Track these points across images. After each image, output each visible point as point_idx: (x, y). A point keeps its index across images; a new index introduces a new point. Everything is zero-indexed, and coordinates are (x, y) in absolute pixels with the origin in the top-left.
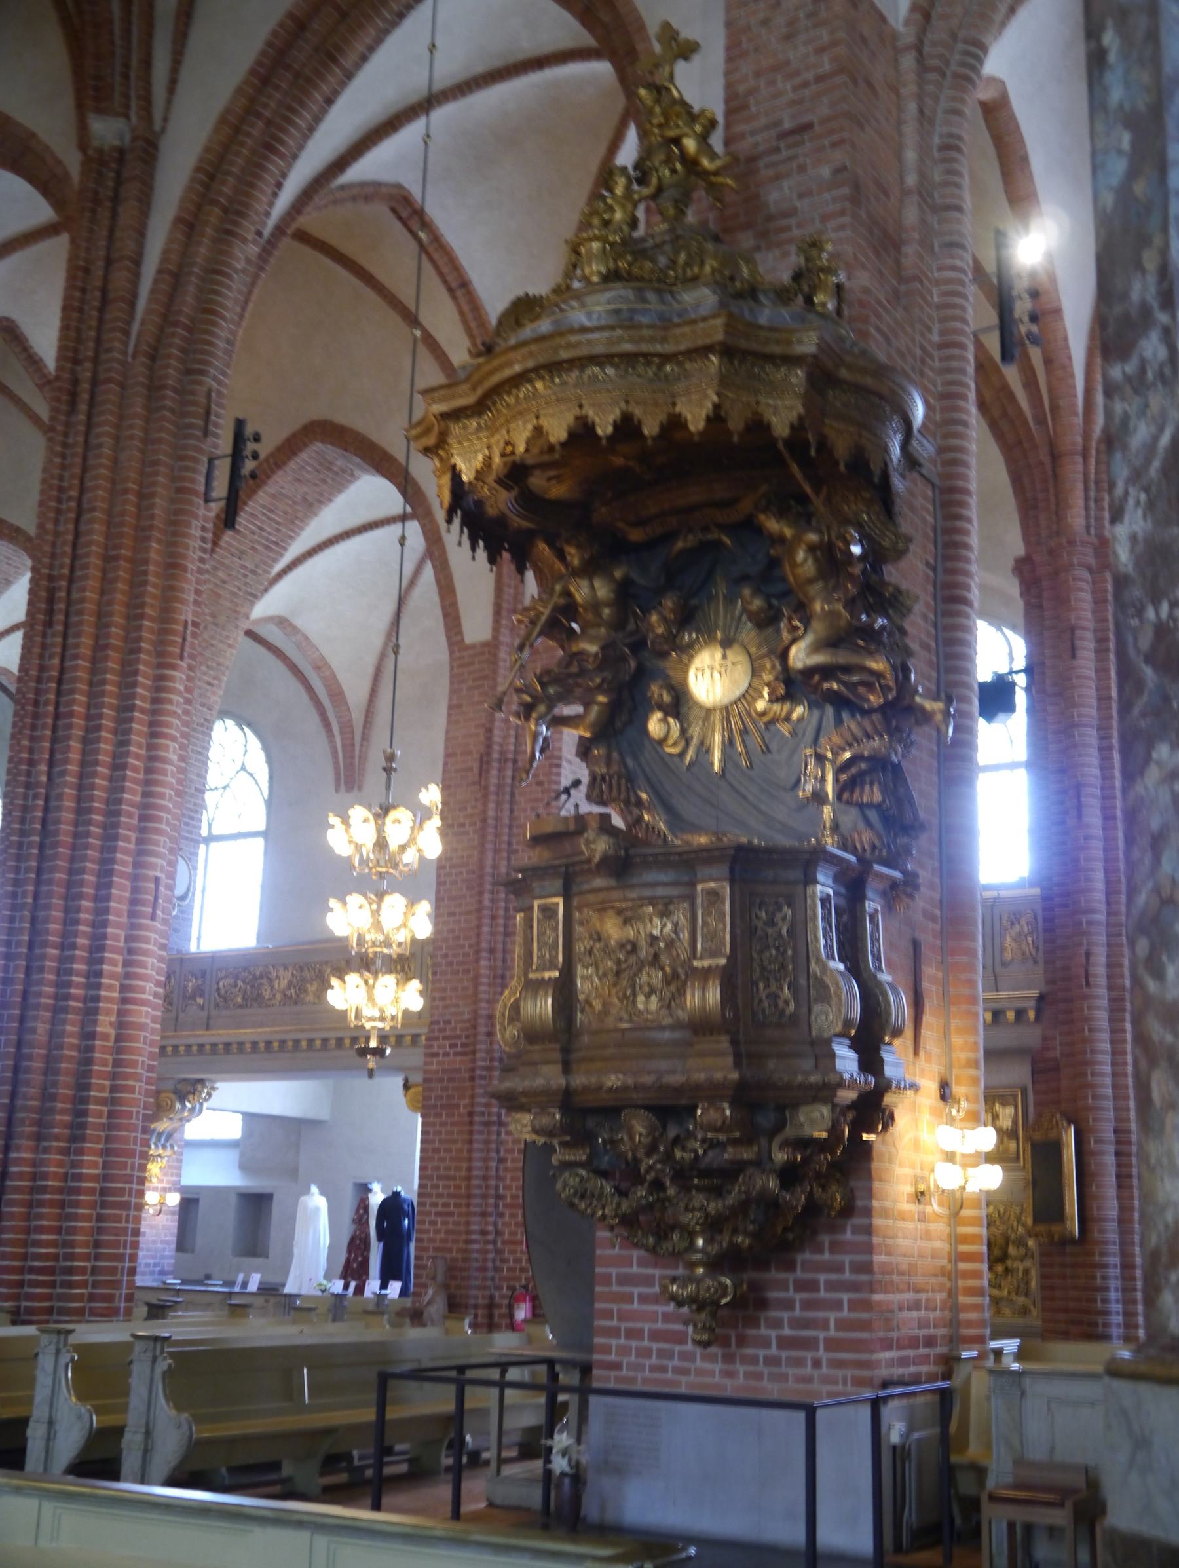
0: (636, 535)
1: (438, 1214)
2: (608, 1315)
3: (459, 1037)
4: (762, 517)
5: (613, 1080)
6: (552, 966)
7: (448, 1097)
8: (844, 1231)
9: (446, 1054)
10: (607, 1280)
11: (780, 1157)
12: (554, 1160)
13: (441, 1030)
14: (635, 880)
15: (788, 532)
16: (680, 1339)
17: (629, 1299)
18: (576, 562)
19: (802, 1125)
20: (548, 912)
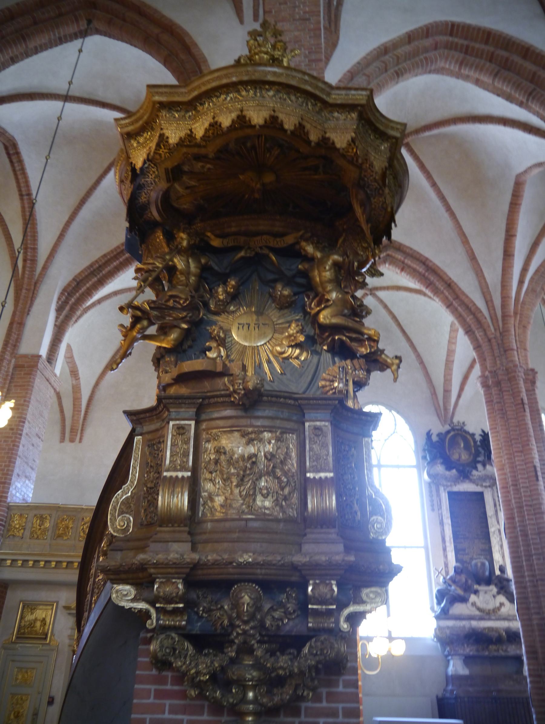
0: (216, 243)
4: (303, 244)
6: (183, 468)
8: (338, 686)
14: (259, 413)
15: (319, 255)
20: (181, 430)
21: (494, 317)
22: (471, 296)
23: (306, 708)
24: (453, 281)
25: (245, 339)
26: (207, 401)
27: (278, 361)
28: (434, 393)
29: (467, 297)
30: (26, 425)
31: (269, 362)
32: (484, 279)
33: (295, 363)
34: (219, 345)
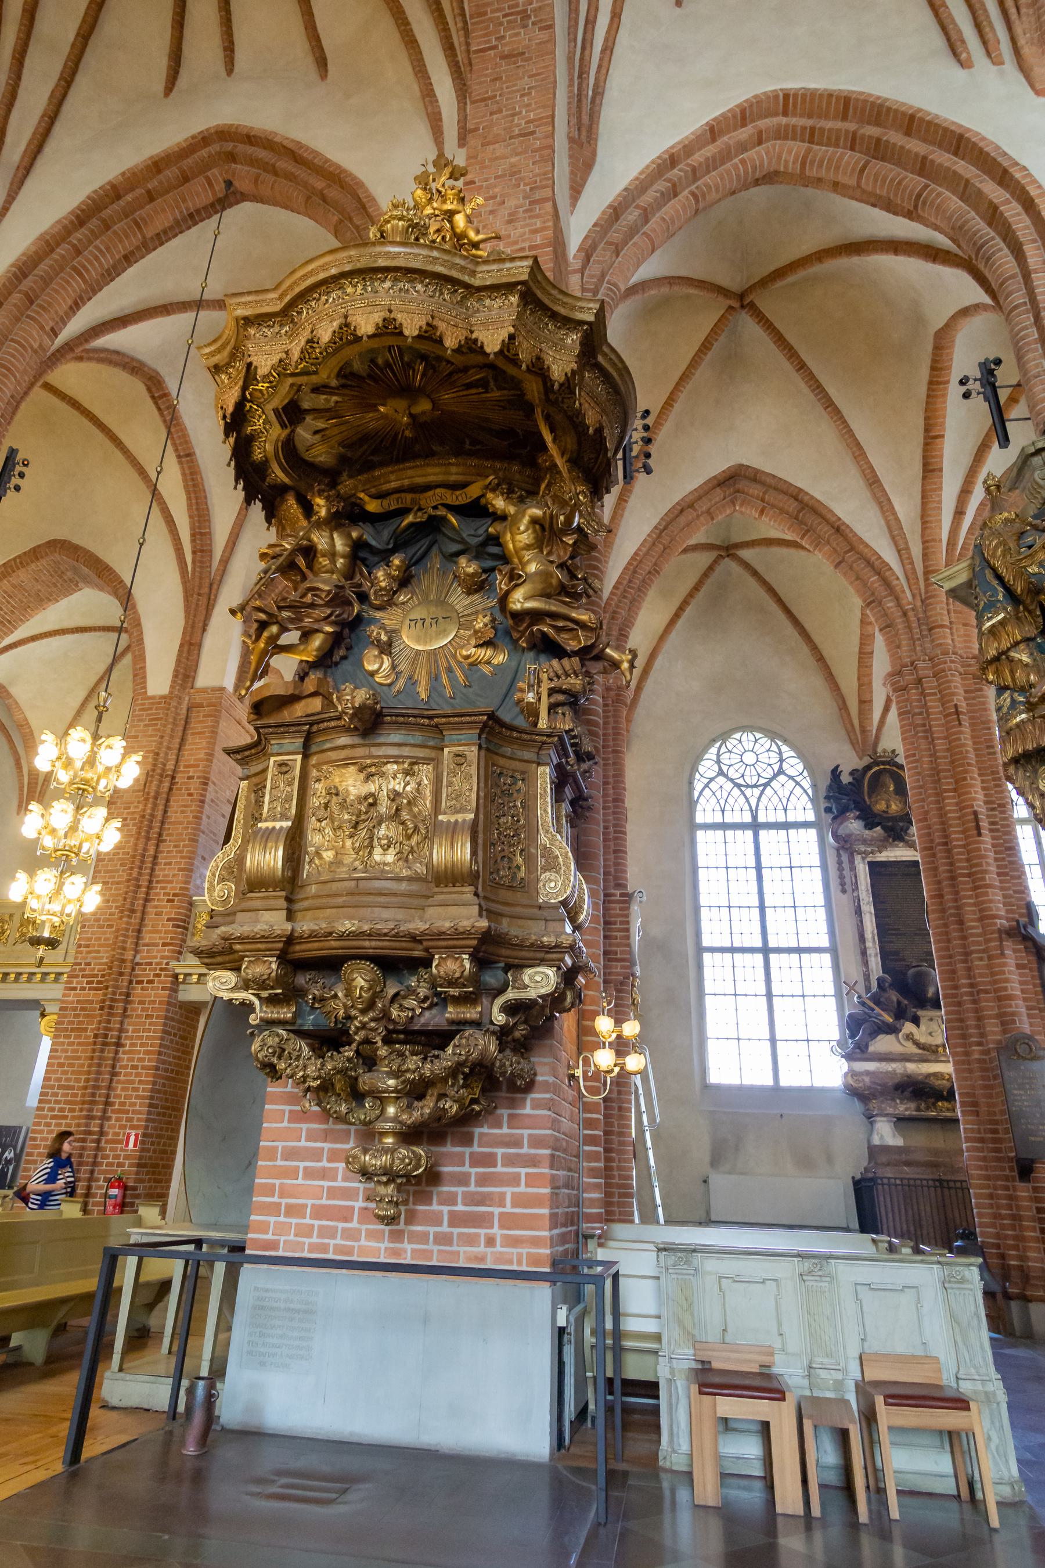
1: (53, 1117)
2: (269, 1190)
3: (96, 976)
5: (347, 925)
6: (284, 817)
7: (79, 1023)
9: (83, 989)
10: (272, 1154)
11: (499, 1018)
12: (254, 1021)
13: (81, 970)
16: (345, 1215)
17: (293, 1173)
18: (323, 512)
19: (526, 987)
20: (284, 767)
21: (910, 575)
22: (873, 544)
23: (481, 1135)
24: (844, 523)
25: (418, 641)
26: (315, 728)
27: (461, 668)
28: (843, 706)
29: (867, 546)
30: (211, 788)
31: (450, 670)
32: (894, 514)
33: (486, 669)
34: (381, 652)
